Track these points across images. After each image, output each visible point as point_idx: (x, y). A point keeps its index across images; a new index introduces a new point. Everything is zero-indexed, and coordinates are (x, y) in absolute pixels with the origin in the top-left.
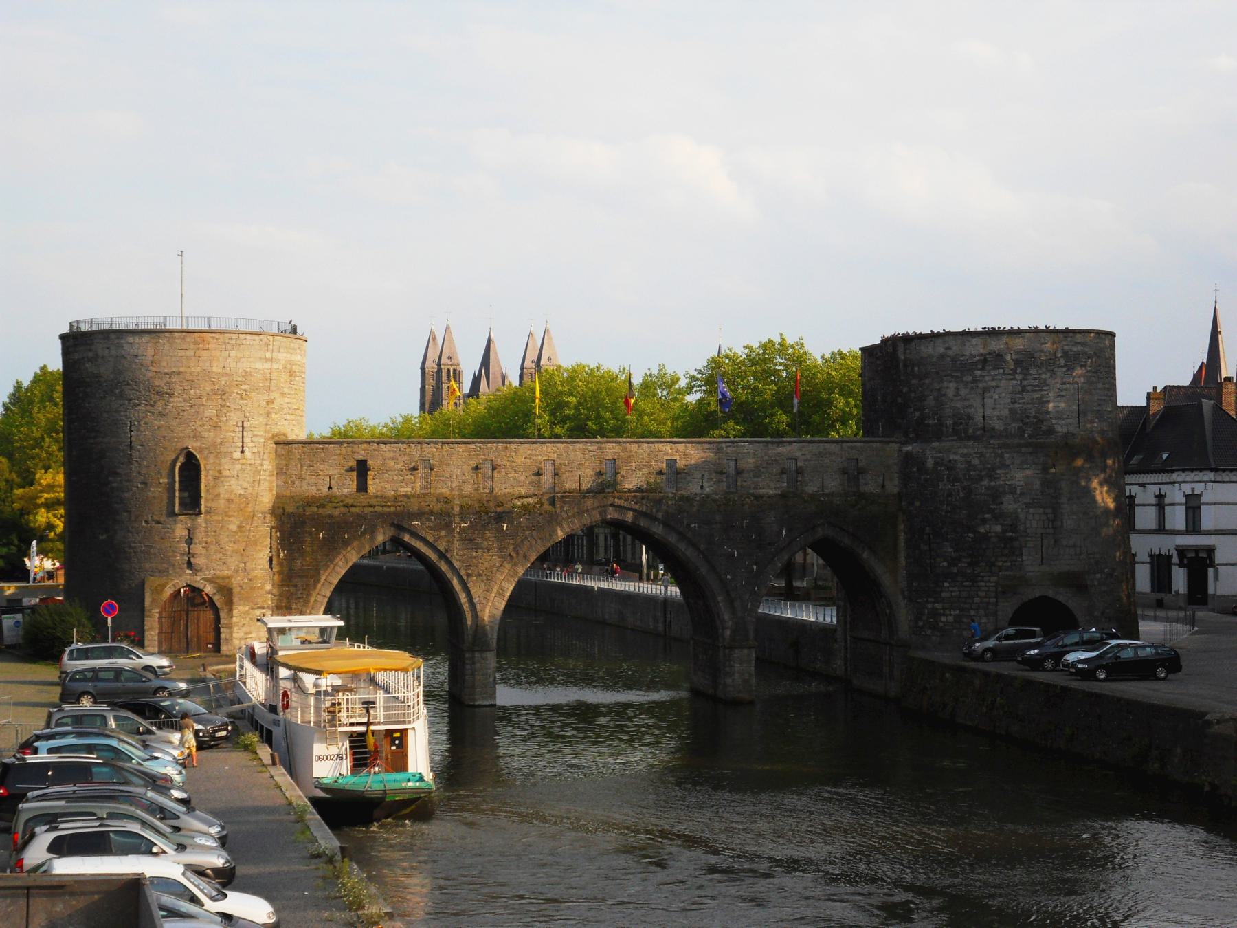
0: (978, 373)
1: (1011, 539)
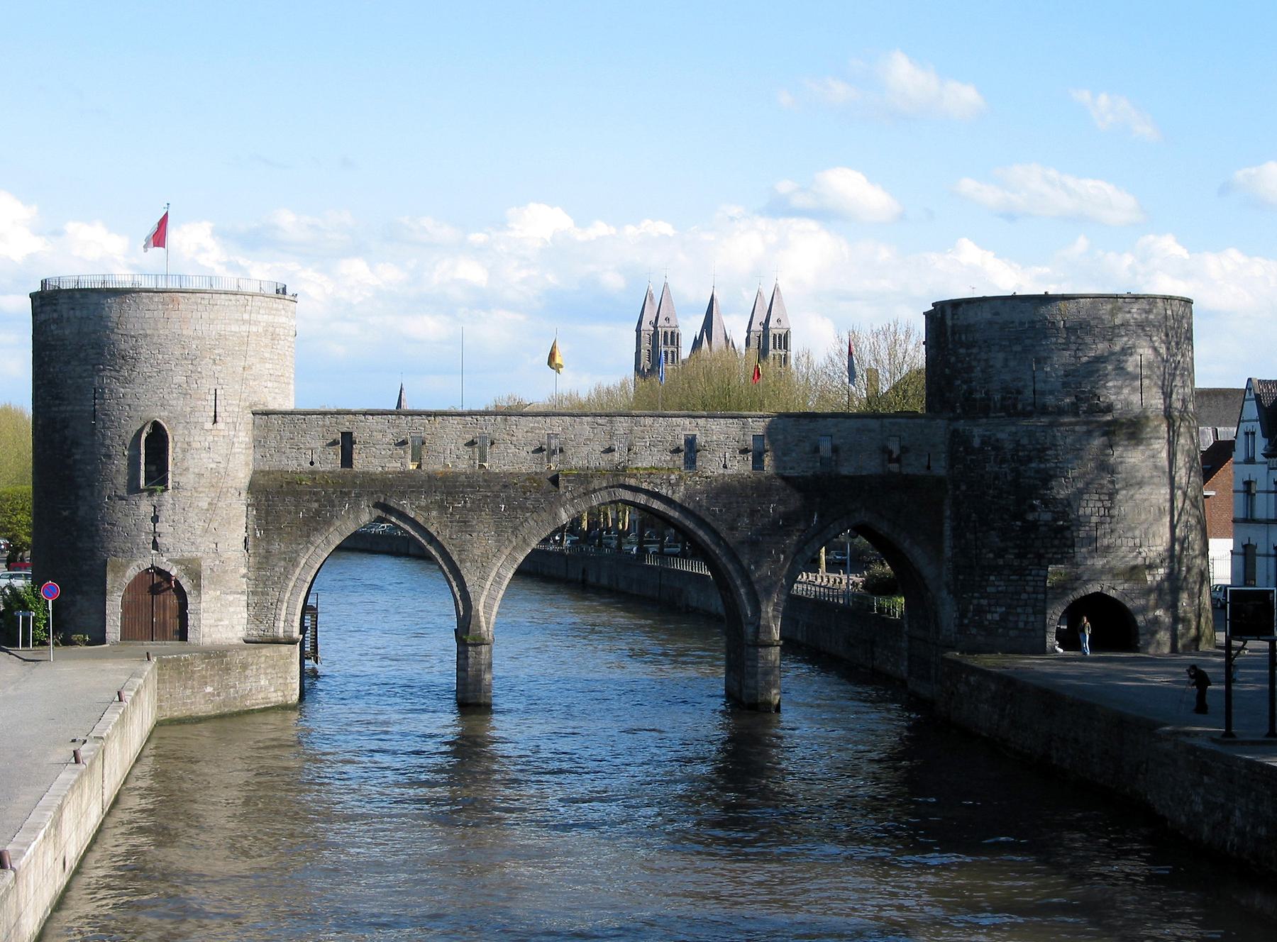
0: (1028, 342)
1: (1062, 528)
